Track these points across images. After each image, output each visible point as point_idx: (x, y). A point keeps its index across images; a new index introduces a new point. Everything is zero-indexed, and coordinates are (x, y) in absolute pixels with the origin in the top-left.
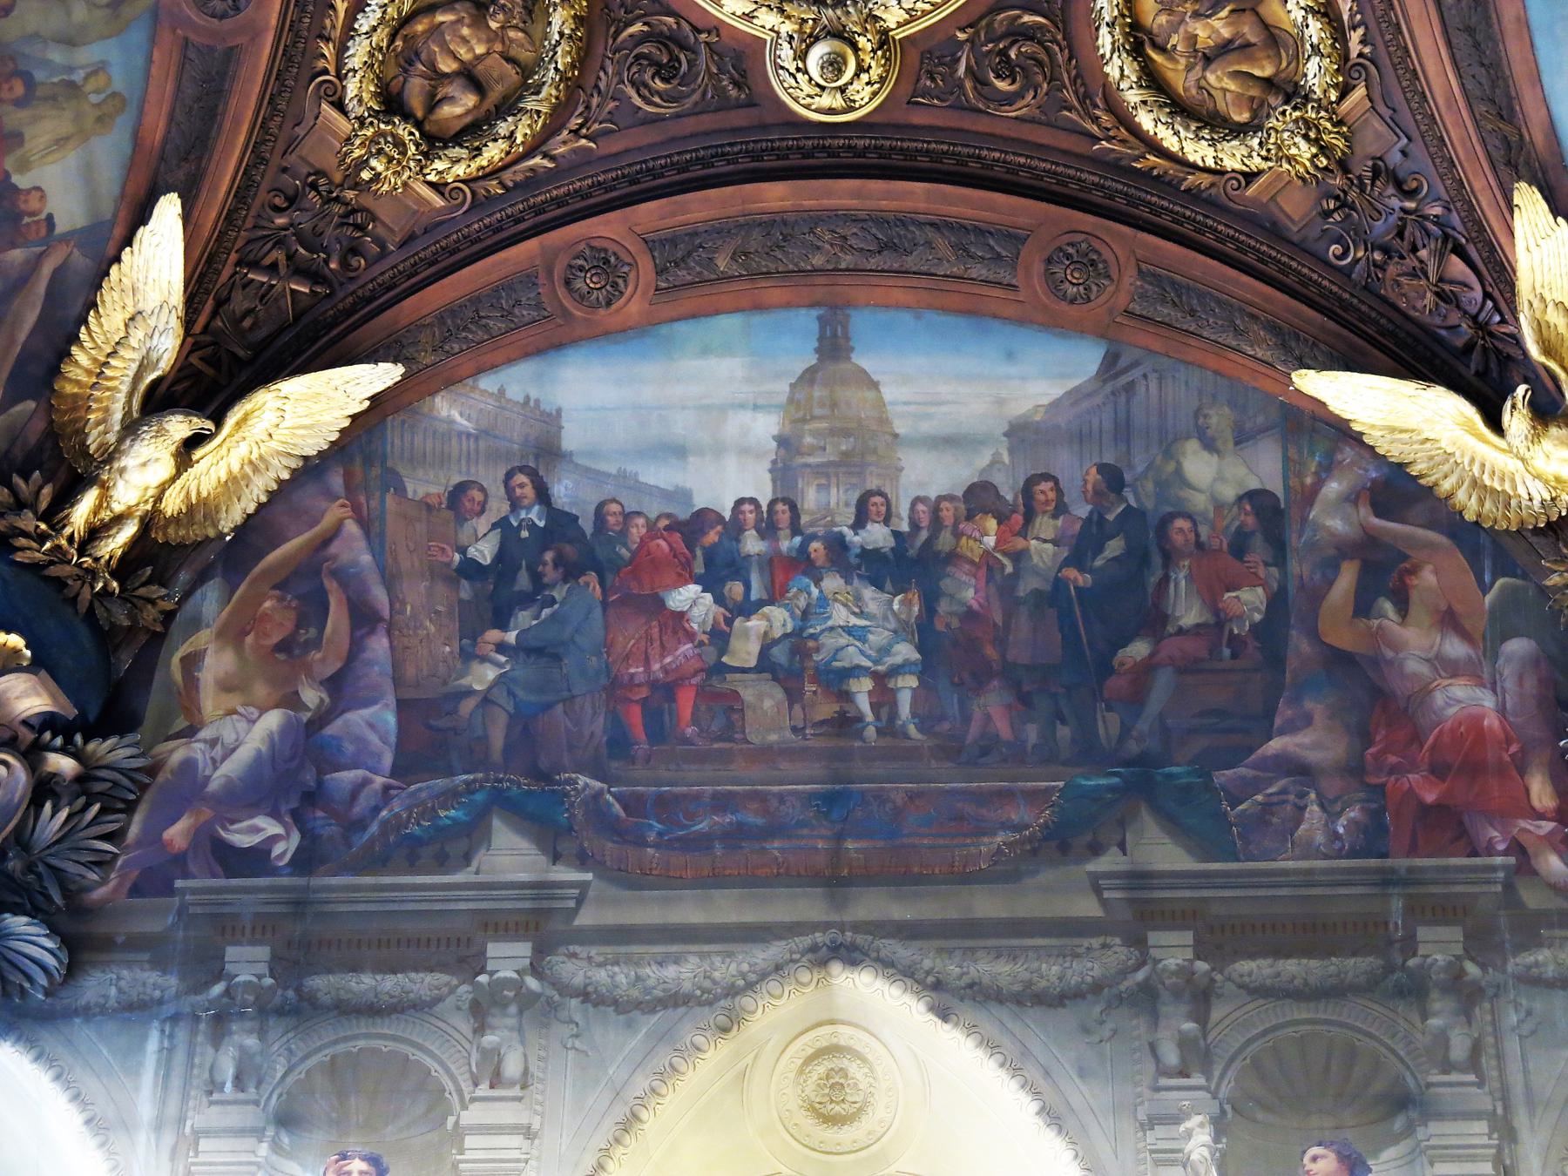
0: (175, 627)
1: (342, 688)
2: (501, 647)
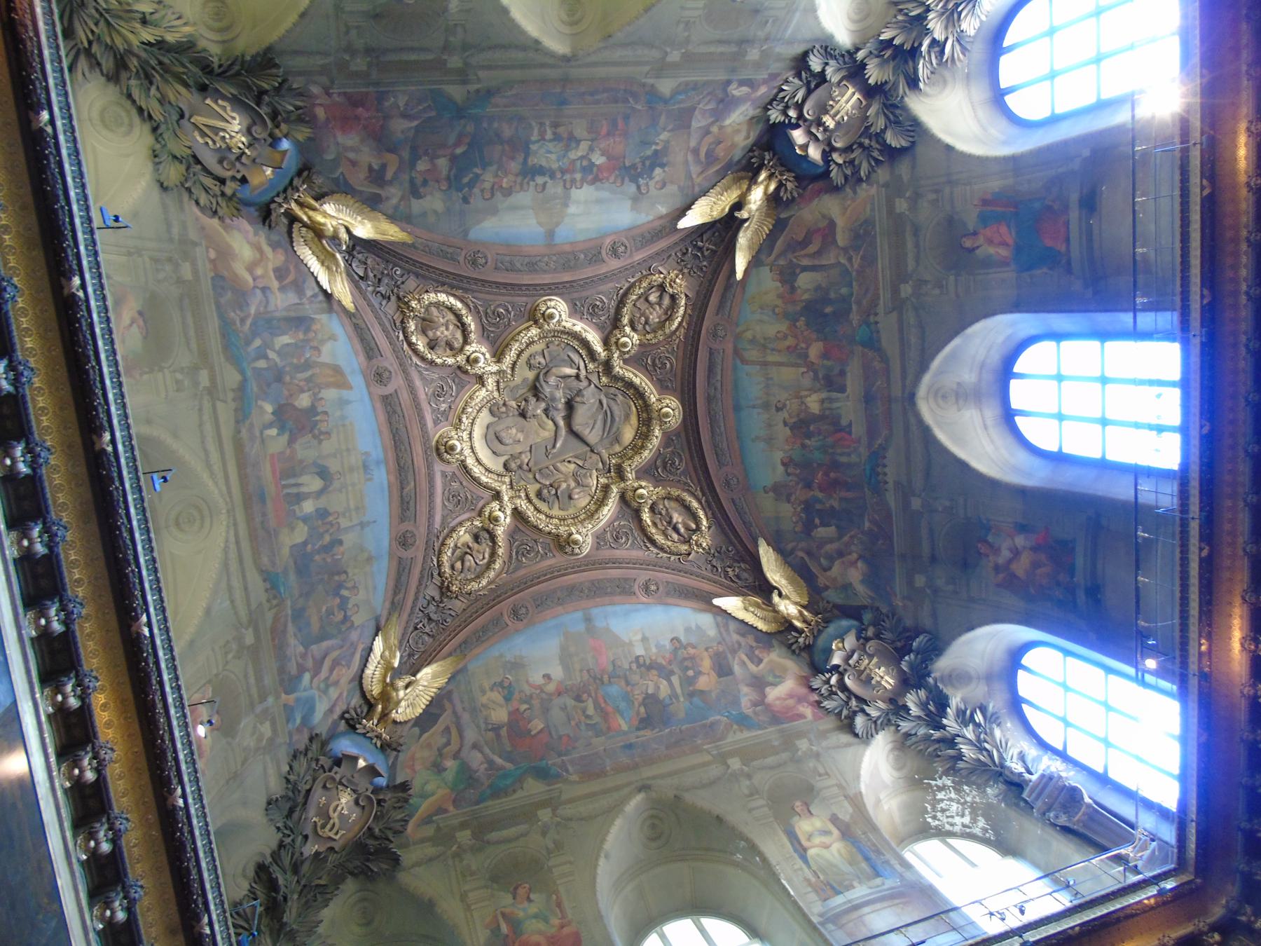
1: (707, 132)
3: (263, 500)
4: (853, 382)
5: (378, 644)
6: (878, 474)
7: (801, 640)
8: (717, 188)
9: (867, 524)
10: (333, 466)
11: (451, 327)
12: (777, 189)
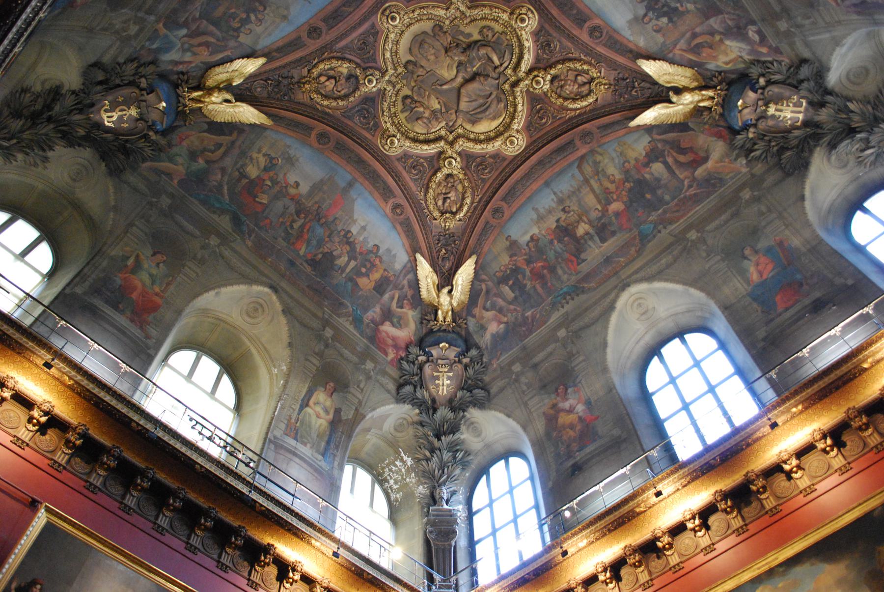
1: (712, 33)
2: (682, 6)
4: (611, 245)
5: (238, 64)
6: (565, 299)
7: (432, 323)
9: (529, 314)
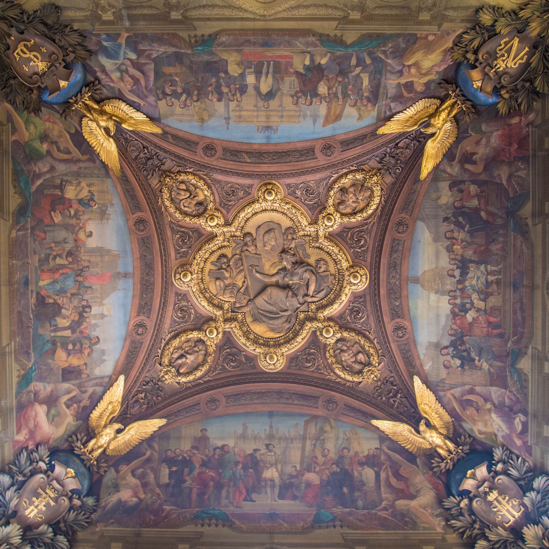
0: (473, 435)
3: (265, 44)
8: (441, 410)
10: (274, 103)
11: (354, 205)
12: (439, 455)
